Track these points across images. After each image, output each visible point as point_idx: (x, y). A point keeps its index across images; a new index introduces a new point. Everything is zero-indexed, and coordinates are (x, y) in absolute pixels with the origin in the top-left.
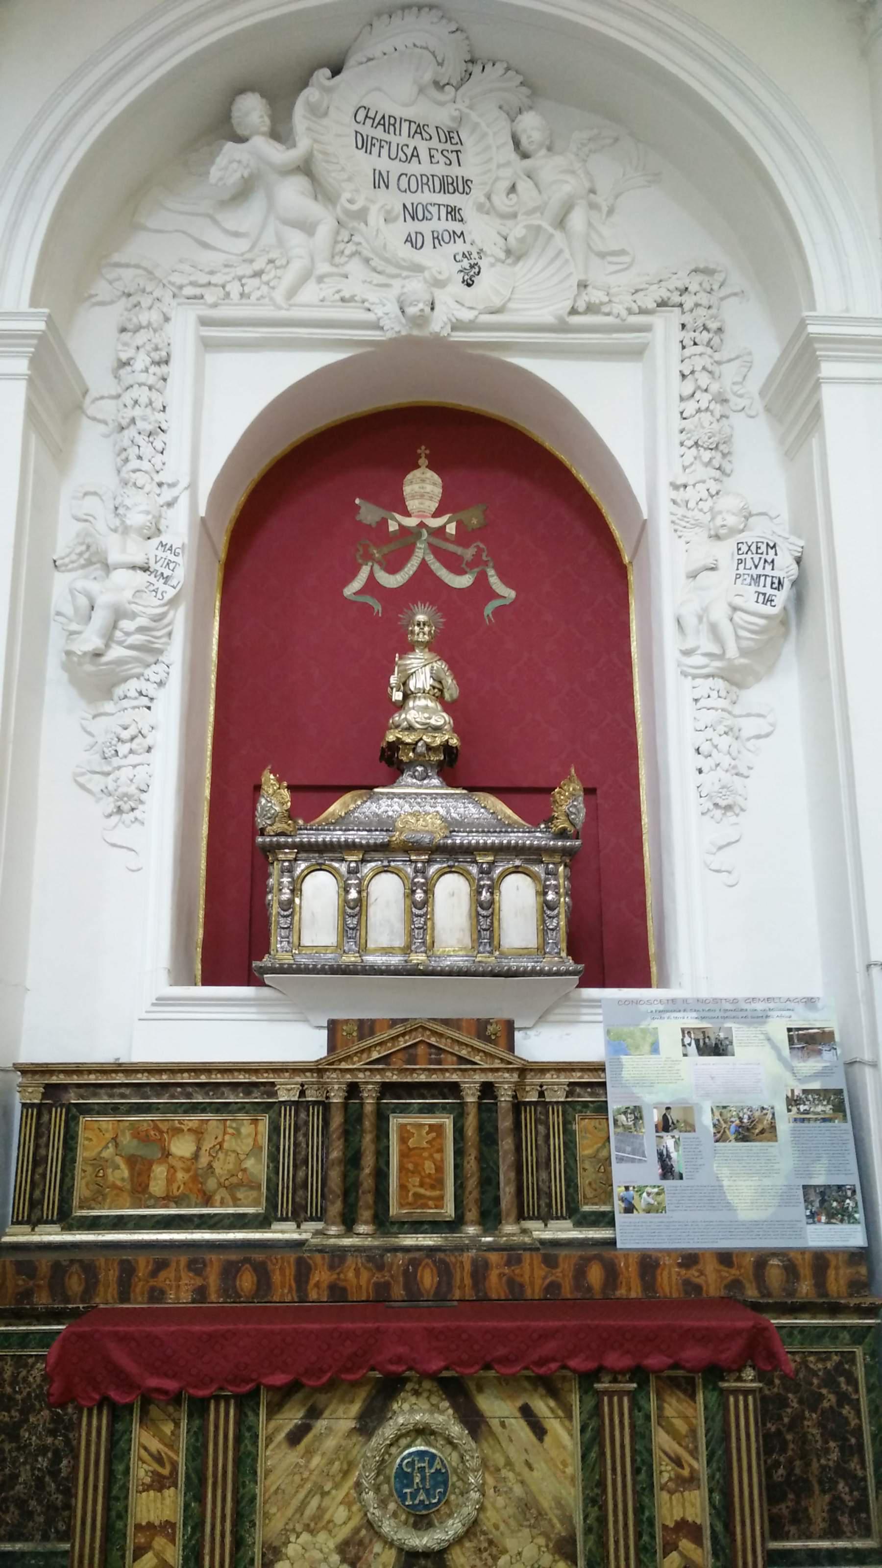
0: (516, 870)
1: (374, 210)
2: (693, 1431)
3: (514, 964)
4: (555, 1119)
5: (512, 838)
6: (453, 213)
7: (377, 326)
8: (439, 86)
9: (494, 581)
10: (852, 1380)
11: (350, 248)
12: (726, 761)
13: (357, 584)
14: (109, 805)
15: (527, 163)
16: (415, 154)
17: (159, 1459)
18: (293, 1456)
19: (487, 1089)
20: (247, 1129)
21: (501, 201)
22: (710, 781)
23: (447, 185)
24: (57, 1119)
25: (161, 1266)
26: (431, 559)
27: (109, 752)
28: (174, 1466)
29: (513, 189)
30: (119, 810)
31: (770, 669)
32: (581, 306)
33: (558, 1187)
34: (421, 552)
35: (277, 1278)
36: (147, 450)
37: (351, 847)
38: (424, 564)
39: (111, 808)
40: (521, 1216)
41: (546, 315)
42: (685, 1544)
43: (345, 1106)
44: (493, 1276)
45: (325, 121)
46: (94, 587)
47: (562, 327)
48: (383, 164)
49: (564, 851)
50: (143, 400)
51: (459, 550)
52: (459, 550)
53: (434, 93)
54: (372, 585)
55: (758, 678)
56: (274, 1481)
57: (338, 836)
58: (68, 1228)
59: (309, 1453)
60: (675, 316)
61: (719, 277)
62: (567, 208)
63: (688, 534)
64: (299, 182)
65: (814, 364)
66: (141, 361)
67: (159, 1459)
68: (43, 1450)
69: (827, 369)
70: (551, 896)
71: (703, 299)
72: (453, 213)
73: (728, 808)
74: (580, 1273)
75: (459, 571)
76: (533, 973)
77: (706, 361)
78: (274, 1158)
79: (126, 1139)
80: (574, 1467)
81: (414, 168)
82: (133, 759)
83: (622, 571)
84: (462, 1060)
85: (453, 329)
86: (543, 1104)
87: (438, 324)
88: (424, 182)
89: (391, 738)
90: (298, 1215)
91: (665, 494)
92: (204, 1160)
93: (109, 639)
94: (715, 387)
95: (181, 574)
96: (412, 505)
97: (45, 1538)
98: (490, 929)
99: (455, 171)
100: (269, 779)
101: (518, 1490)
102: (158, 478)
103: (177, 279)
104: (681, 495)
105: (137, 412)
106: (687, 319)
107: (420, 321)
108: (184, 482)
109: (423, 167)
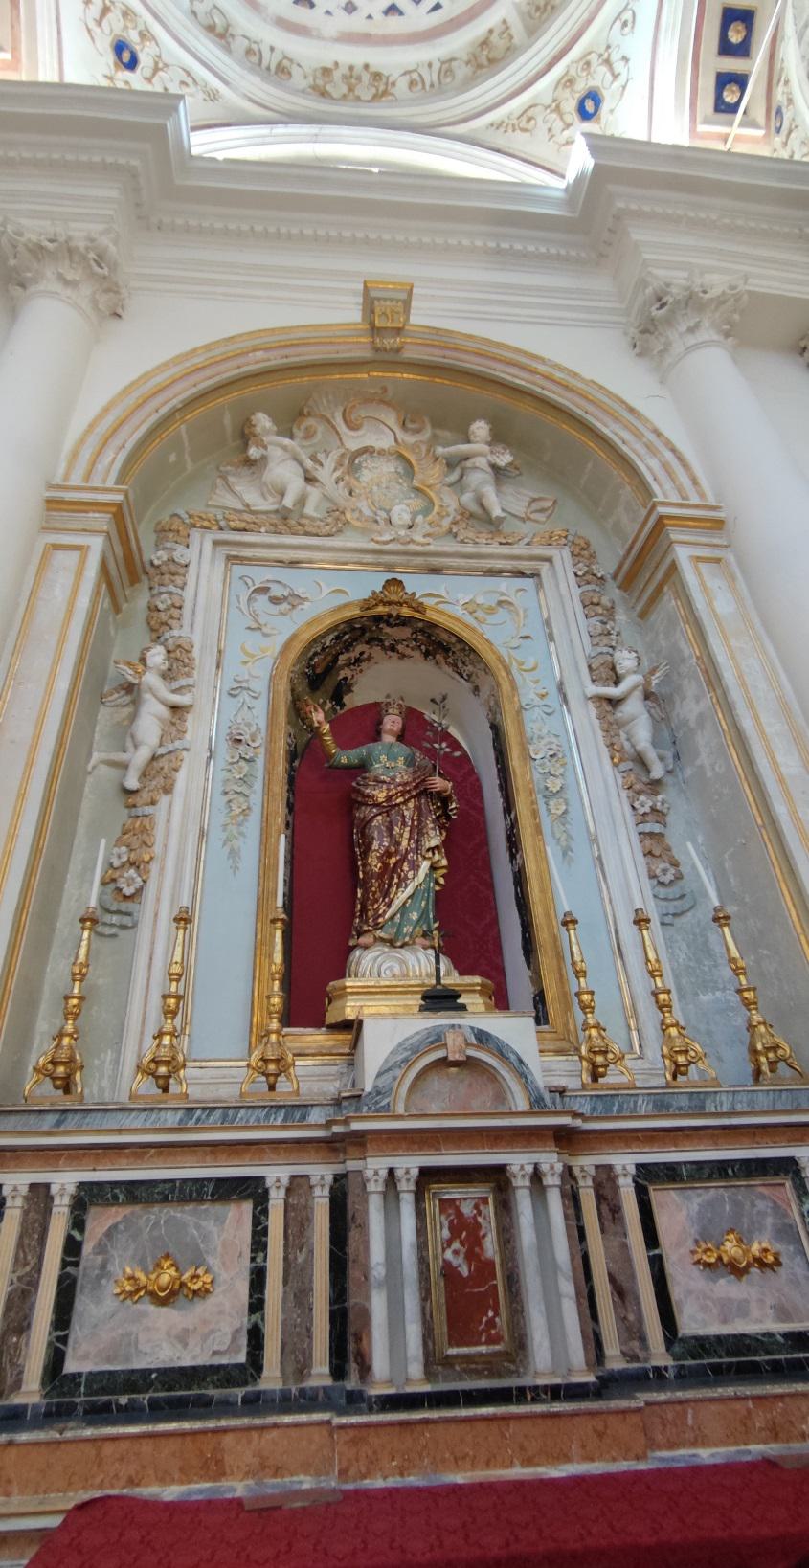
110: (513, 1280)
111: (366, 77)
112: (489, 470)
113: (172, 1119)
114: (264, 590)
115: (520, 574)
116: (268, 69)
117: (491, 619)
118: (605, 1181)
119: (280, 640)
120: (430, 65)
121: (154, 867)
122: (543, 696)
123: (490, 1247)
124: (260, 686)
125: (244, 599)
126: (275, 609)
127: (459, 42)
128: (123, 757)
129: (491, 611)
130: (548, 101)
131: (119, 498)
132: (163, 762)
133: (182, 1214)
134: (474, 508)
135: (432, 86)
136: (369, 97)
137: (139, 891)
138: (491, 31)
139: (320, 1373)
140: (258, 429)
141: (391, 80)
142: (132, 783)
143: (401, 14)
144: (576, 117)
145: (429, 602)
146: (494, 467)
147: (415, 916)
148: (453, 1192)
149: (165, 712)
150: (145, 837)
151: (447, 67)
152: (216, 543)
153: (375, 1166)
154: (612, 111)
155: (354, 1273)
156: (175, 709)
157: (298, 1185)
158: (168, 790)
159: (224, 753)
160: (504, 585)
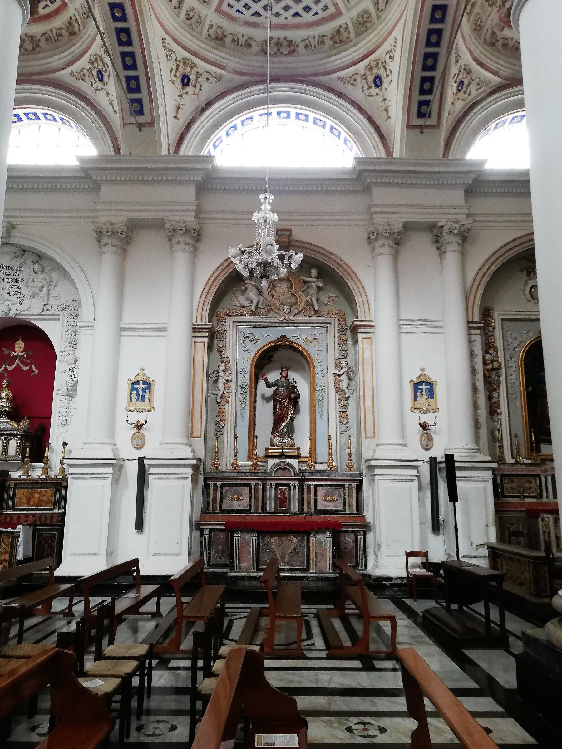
6: (19, 287)
8: (16, 257)
9: (34, 368)
10: (55, 538)
16: (10, 274)
21: (30, 284)
23: (18, 281)
26: (19, 363)
29: (34, 281)
32: (45, 309)
34: (18, 360)
38: (18, 364)
42: (5, 563)
51: (26, 361)
52: (26, 361)
53: (15, 259)
60: (66, 312)
61: (78, 303)
71: (73, 308)
72: (19, 287)
75: (26, 366)
81: (10, 277)
87: (11, 314)
88: (12, 280)
96: (16, 350)
99: (20, 277)
109: (11, 277)
110: (290, 500)
111: (285, 43)
112: (316, 288)
114: (248, 337)
115: (321, 327)
116: (242, 45)
117: (311, 344)
118: (309, 487)
119: (253, 354)
120: (314, 37)
121: (226, 421)
122: (322, 371)
123: (286, 495)
124: (248, 370)
125: (242, 340)
126: (251, 343)
127: (327, 28)
128: (217, 393)
129: (311, 342)
130: (362, 73)
131: (210, 327)
132: (225, 395)
133: (238, 488)
134: (310, 302)
135: (315, 47)
136: (286, 53)
137: (223, 427)
138: (341, 26)
139: (260, 510)
141: (296, 44)
142: (219, 400)
143: (300, 16)
144: (373, 86)
145: (293, 339)
146: (318, 287)
147: (285, 430)
148: (281, 487)
151: (321, 40)
152: (233, 322)
153: (269, 483)
154: (386, 89)
155: (265, 498)
156: (227, 381)
157: (257, 485)
158: (227, 402)
159: (239, 391)
160: (316, 331)
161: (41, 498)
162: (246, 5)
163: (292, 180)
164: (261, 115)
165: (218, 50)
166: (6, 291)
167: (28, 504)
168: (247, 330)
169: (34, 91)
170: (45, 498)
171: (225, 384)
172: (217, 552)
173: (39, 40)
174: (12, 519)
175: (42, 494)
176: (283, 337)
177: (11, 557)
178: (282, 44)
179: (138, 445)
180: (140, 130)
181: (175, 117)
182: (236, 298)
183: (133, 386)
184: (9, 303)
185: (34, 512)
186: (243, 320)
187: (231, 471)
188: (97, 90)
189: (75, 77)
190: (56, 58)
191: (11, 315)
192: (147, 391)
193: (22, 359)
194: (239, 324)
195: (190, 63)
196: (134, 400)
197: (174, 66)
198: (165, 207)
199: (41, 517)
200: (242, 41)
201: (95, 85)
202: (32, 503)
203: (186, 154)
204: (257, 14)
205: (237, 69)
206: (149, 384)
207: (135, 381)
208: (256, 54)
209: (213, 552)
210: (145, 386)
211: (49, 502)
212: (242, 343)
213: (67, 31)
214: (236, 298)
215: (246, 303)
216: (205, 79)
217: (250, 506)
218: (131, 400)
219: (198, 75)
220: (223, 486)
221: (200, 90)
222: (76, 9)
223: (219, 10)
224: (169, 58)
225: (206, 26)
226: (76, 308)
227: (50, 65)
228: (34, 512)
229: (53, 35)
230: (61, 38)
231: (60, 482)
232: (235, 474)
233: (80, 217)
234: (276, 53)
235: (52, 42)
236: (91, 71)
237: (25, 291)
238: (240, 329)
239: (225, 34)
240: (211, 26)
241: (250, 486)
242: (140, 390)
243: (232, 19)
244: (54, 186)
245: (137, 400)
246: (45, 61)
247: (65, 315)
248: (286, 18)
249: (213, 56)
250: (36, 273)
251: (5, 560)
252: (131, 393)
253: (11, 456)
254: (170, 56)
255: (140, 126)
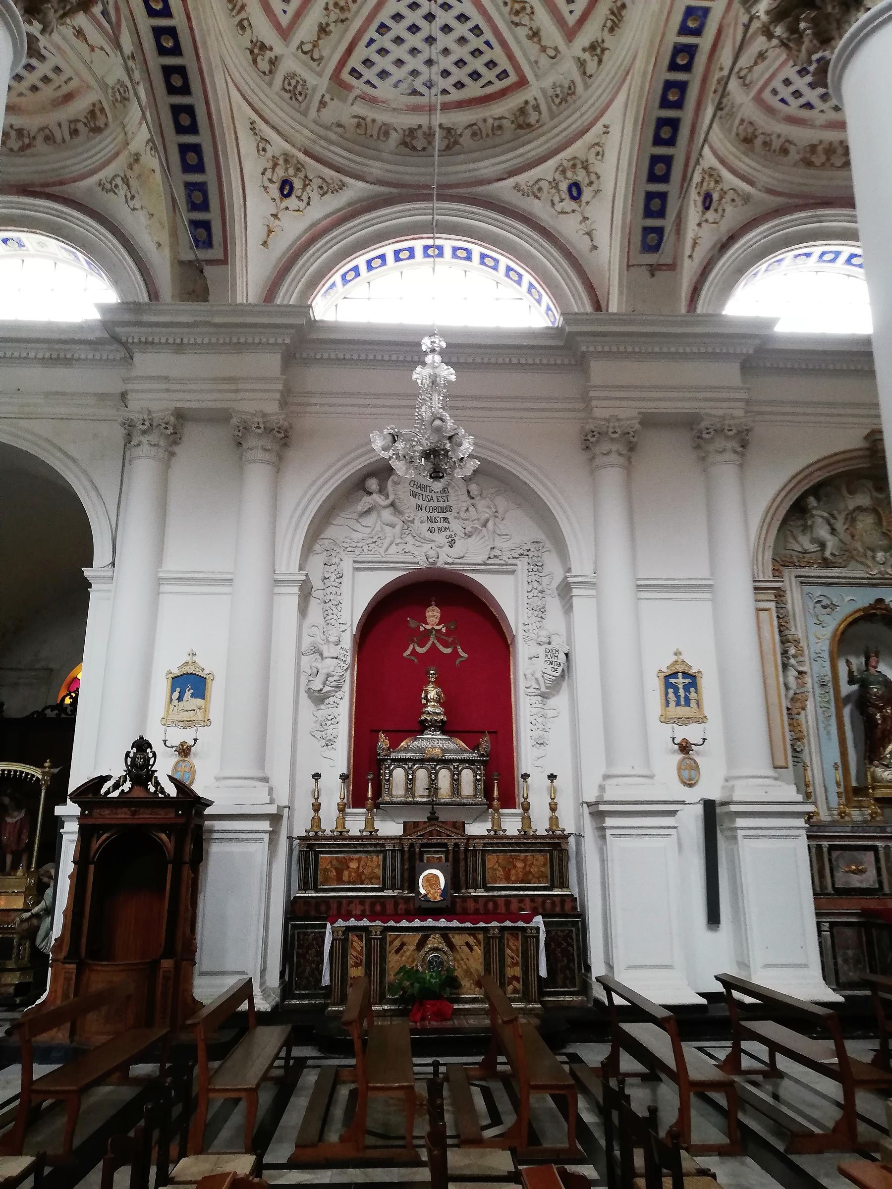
0: (467, 768)
1: (417, 519)
2: (517, 949)
3: (465, 801)
4: (479, 855)
5: (466, 756)
6: (446, 520)
7: (417, 563)
9: (460, 650)
10: (572, 939)
11: (408, 531)
12: (541, 727)
13: (408, 652)
14: (323, 742)
15: (473, 501)
17: (356, 957)
18: (397, 957)
19: (457, 845)
20: (375, 859)
21: (463, 514)
22: (536, 734)
23: (443, 510)
24: (312, 856)
25: (350, 903)
26: (436, 641)
27: (323, 724)
28: (361, 960)
30: (327, 745)
31: (558, 692)
33: (480, 878)
34: (432, 639)
35: (388, 907)
36: (335, 611)
37: (410, 760)
38: (433, 643)
39: (324, 744)
40: (467, 888)
41: (479, 560)
42: (514, 983)
43: (409, 850)
44: (458, 905)
45: (399, 486)
46: (319, 665)
47: (485, 564)
48: (420, 502)
49: (483, 762)
50: (334, 593)
51: (447, 638)
52: (447, 638)
54: (414, 652)
55: (554, 695)
56: (391, 965)
57: (403, 755)
58: (316, 891)
59: (402, 956)
60: (525, 559)
62: (487, 521)
63: (529, 642)
64: (391, 509)
65: (571, 589)
66: (333, 577)
67: (356, 957)
68: (313, 962)
69: (575, 592)
70: (478, 777)
71: (536, 554)
72: (446, 520)
73: (542, 744)
74: (486, 904)
75: (447, 647)
76: (472, 804)
77: (536, 578)
78: (384, 869)
79: (335, 862)
80: (481, 960)
81: (431, 504)
82: (332, 727)
83: (507, 647)
84: (448, 835)
85: (446, 564)
86: (475, 851)
87: (440, 564)
88: (435, 509)
89: (423, 718)
90: (393, 888)
91: (521, 627)
92: (361, 870)
93: (324, 684)
94: (540, 588)
95: (349, 660)
96: (429, 620)
97: (315, 989)
98: (458, 789)
99: (447, 504)
100: (382, 736)
101: (465, 967)
102: (339, 621)
103: (345, 545)
104: (526, 628)
105: (332, 597)
106: (530, 561)
107: (434, 563)
108: (349, 624)
109: (435, 504)
113: (849, 829)
121: (806, 741)
125: (811, 607)
126: (825, 611)
133: (855, 853)
140: (809, 507)
149: (796, 674)
150: (799, 728)
156: (800, 673)
158: (804, 709)
161: (528, 869)
162: (797, 91)
163: (793, 351)
164: (796, 256)
165: (747, 156)
166: (427, 525)
167: (508, 878)
168: (818, 591)
169: (465, 214)
170: (534, 870)
171: (797, 678)
172: (846, 961)
173: (460, 135)
174: (496, 904)
175: (529, 863)
176: (880, 601)
177: (525, 972)
178: (834, 152)
179: (690, 780)
180: (653, 275)
181: (265, 244)
182: (795, 538)
183: (668, 680)
184: (433, 545)
185: (522, 893)
186: (813, 574)
187: (833, 823)
188: (563, 212)
189: (521, 193)
190: (487, 163)
191: (439, 565)
192: (692, 690)
193: (438, 635)
194: (804, 581)
195: (715, 175)
196: (672, 704)
197: (270, 164)
198: (698, 395)
199: (544, 903)
200: (776, 144)
201: (559, 207)
202: (513, 879)
203: (285, 302)
204: (808, 106)
205: (770, 187)
206: (693, 677)
207: (670, 672)
208: (795, 164)
209: (840, 961)
210: (687, 681)
211: (541, 877)
212: (811, 611)
213: (513, 122)
214: (795, 538)
215: (812, 548)
216: (729, 200)
217: (880, 882)
218: (667, 703)
219: (723, 193)
220: (831, 848)
221: (723, 216)
222: (542, 89)
223: (758, 99)
224: (262, 153)
225: (737, 121)
226: (539, 554)
227: (365, 168)
228: (522, 893)
229: (486, 129)
230: (499, 132)
231: (557, 841)
232: (849, 829)
233: (551, 410)
234: (823, 164)
235: (482, 138)
236: (557, 184)
237: (456, 526)
238: (807, 588)
239: (757, 133)
240: (742, 121)
241: (875, 849)
242: (681, 686)
243: (770, 111)
244: (507, 361)
245: (678, 704)
246: (471, 166)
247: (522, 565)
248: (822, 111)
249: (741, 164)
250: (472, 498)
251: (515, 978)
252: (667, 694)
253: (468, 797)
254: (264, 150)
255: (653, 270)
